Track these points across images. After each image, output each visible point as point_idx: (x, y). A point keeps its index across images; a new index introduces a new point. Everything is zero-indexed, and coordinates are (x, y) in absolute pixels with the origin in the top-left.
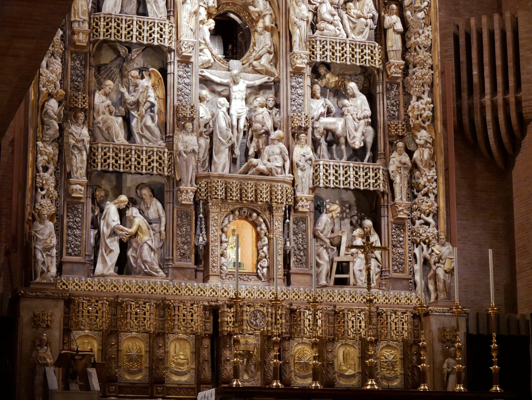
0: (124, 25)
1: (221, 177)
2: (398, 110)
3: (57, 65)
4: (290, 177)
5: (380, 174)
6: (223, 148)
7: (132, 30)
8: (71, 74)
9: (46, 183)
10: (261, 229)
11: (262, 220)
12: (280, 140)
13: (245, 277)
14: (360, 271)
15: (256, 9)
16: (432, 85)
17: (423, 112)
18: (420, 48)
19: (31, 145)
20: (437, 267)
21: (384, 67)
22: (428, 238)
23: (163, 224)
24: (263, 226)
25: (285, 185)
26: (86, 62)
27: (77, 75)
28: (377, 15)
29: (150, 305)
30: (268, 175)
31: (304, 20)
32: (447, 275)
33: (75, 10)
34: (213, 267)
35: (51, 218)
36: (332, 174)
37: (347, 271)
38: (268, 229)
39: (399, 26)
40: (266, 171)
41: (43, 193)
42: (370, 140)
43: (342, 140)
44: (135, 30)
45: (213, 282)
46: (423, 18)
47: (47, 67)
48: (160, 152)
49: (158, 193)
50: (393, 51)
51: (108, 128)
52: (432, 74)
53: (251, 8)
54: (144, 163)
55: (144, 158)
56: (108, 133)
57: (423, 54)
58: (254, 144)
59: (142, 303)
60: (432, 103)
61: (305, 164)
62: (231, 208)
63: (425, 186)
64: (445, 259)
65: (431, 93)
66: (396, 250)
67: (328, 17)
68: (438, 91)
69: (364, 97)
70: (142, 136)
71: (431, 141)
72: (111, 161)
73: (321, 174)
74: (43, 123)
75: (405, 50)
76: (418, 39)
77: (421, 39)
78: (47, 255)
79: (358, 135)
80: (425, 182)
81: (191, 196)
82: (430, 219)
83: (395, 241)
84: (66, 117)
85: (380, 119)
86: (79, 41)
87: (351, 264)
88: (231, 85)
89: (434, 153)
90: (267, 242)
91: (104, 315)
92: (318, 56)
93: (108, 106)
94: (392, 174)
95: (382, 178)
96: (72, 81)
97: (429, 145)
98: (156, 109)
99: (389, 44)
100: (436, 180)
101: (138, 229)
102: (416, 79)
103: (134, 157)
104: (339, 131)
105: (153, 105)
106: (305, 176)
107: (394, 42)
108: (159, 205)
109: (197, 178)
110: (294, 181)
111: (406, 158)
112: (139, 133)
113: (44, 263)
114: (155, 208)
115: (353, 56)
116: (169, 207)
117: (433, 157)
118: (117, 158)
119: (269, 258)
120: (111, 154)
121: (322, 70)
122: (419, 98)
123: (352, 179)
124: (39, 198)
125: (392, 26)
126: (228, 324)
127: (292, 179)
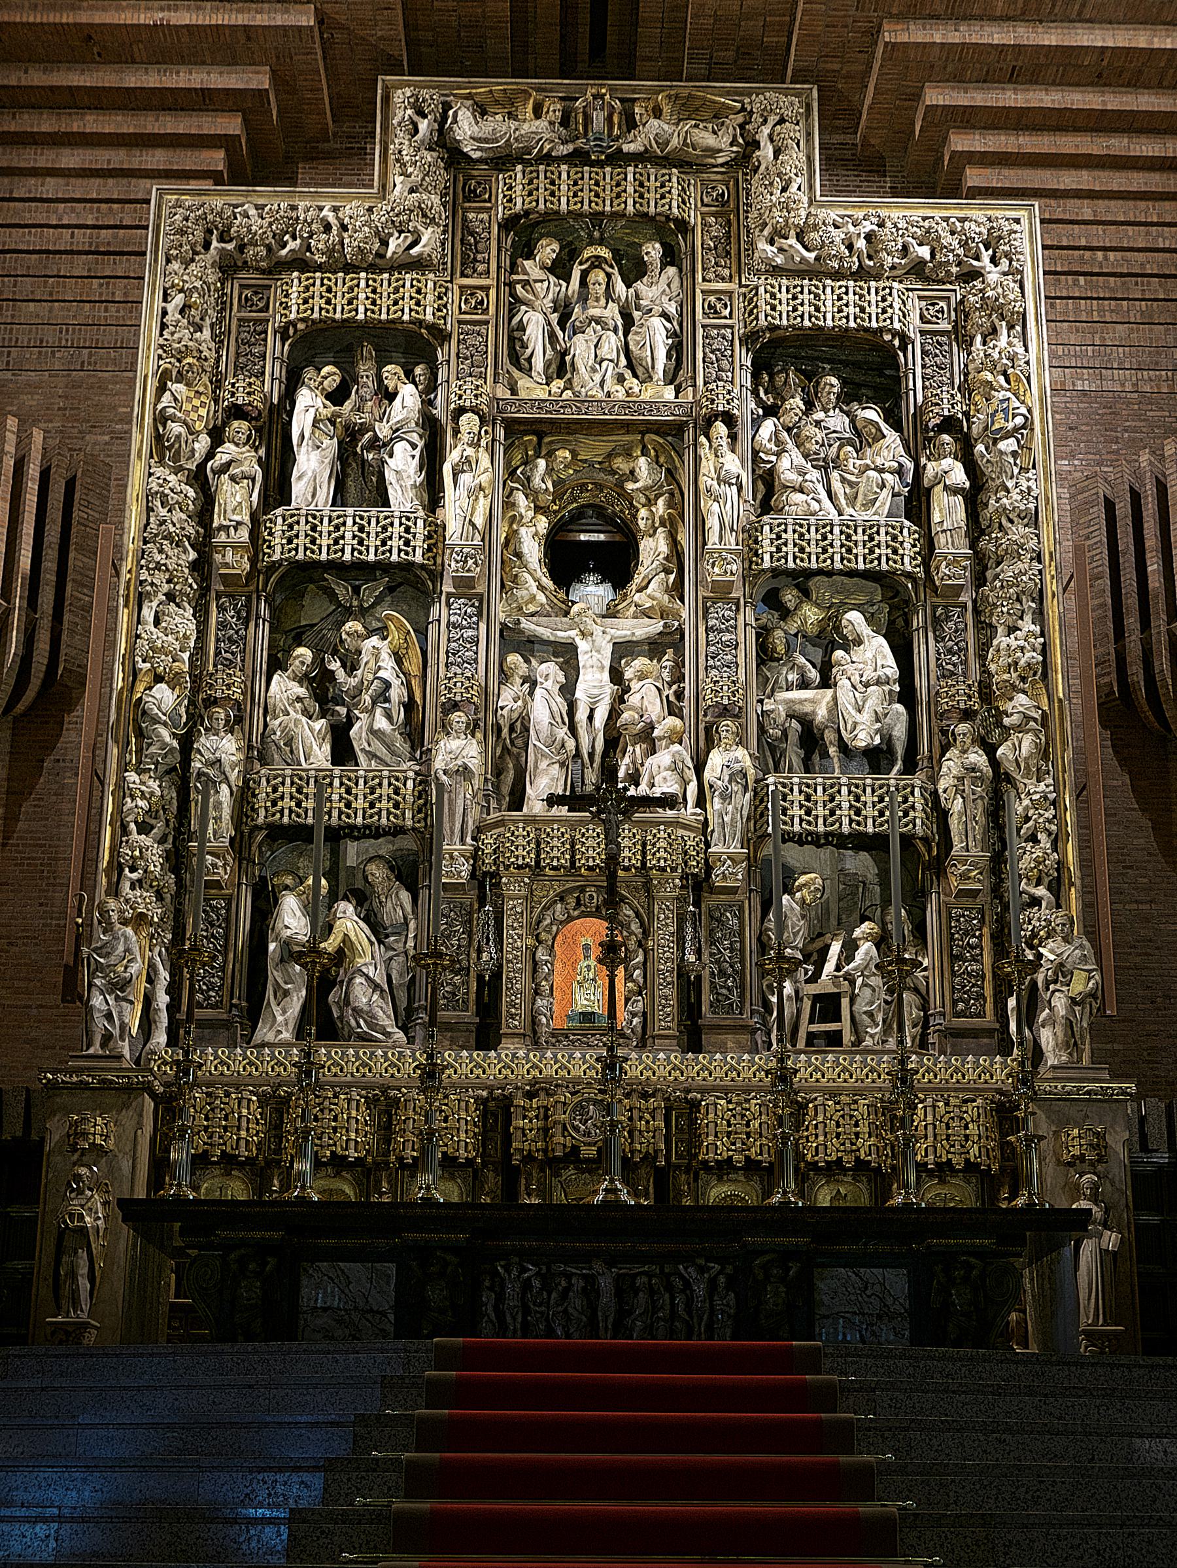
0: (325, 527)
1: (531, 820)
2: (965, 663)
3: (184, 620)
4: (695, 814)
5: (917, 799)
7: (343, 537)
8: (218, 640)
9: (141, 857)
12: (675, 738)
14: (870, 1014)
15: (638, 485)
16: (1040, 598)
17: (1019, 654)
18: (1012, 522)
19: (112, 780)
20: (1053, 992)
21: (927, 571)
22: (1034, 935)
23: (411, 935)
25: (680, 832)
26: (248, 613)
27: (231, 640)
28: (909, 465)
29: (349, 1101)
31: (730, 485)
32: (1077, 1008)
33: (220, 505)
34: (512, 1016)
35: (140, 920)
36: (796, 804)
37: (838, 1019)
39: (959, 476)
41: (135, 876)
42: (900, 732)
43: (829, 736)
44: (348, 535)
46: (1014, 454)
47: (157, 622)
48: (397, 779)
49: (410, 872)
50: (944, 531)
51: (289, 743)
52: (1040, 571)
53: (630, 486)
54: (360, 804)
55: (360, 793)
56: (292, 752)
57: (1018, 532)
59: (330, 1095)
60: (1042, 634)
62: (558, 888)
63: (1027, 819)
64: (1072, 973)
65: (1040, 616)
66: (960, 967)
67: (791, 477)
68: (1053, 609)
69: (882, 640)
70: (372, 756)
71: (1037, 715)
72: (287, 803)
74: (140, 734)
75: (976, 528)
76: (1005, 500)
77: (1012, 500)
78: (117, 998)
79: (866, 717)
80: (1027, 808)
81: (465, 868)
82: (1041, 891)
83: (958, 946)
84: (194, 719)
85: (921, 683)
86: (226, 565)
87: (845, 1002)
88: (578, 641)
89: (1047, 743)
91: (244, 1124)
92: (767, 557)
93: (299, 699)
94: (943, 796)
95: (918, 806)
96: (218, 653)
98: (397, 693)
99: (936, 517)
100: (1054, 803)
101: (344, 941)
102: (1002, 587)
103: (337, 791)
104: (822, 713)
105: (387, 685)
107: (948, 512)
108: (405, 896)
109: (479, 830)
110: (706, 823)
111: (977, 757)
112: (363, 750)
113: (109, 1016)
114: (397, 904)
115: (849, 551)
116: (423, 894)
117: (1044, 753)
118: (302, 797)
120: (287, 789)
121: (789, 597)
122: (1011, 630)
123: (844, 812)
124: (126, 887)
125: (939, 479)
126: (524, 1135)
127: (701, 818)
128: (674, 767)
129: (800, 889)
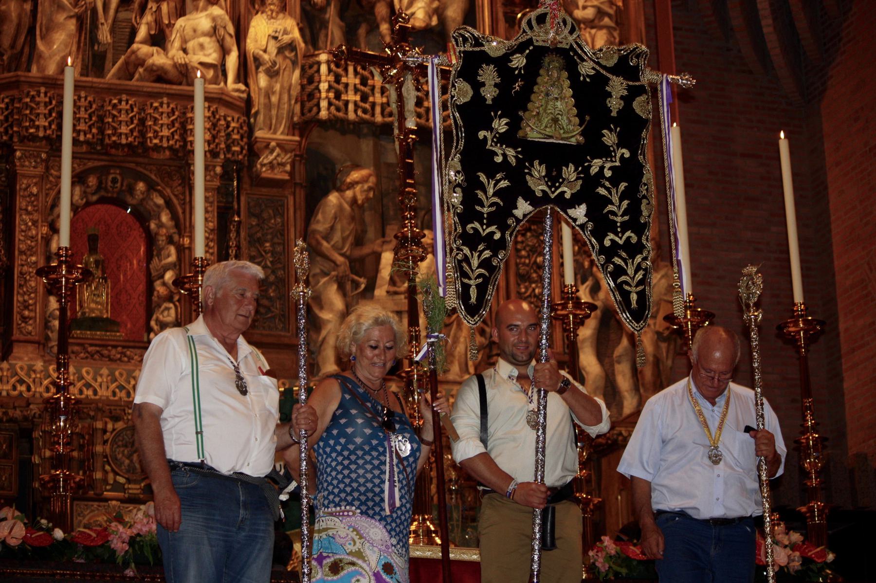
4: (238, 90)
6: (61, 17)
10: (161, 225)
11: (160, 201)
13: (113, 352)
24: (165, 218)
30: (180, 84)
34: (25, 319)
36: (351, 88)
38: (177, 226)
40: (173, 73)
45: (21, 359)
58: (148, 18)
61: (279, 60)
66: (527, 288)
73: (324, 86)
83: (524, 264)
90: (173, 258)
97: (606, 21)
106: (277, 87)
110: (249, 102)
119: (179, 301)
127: (244, 96)
128: (214, 31)
129: (352, 185)
